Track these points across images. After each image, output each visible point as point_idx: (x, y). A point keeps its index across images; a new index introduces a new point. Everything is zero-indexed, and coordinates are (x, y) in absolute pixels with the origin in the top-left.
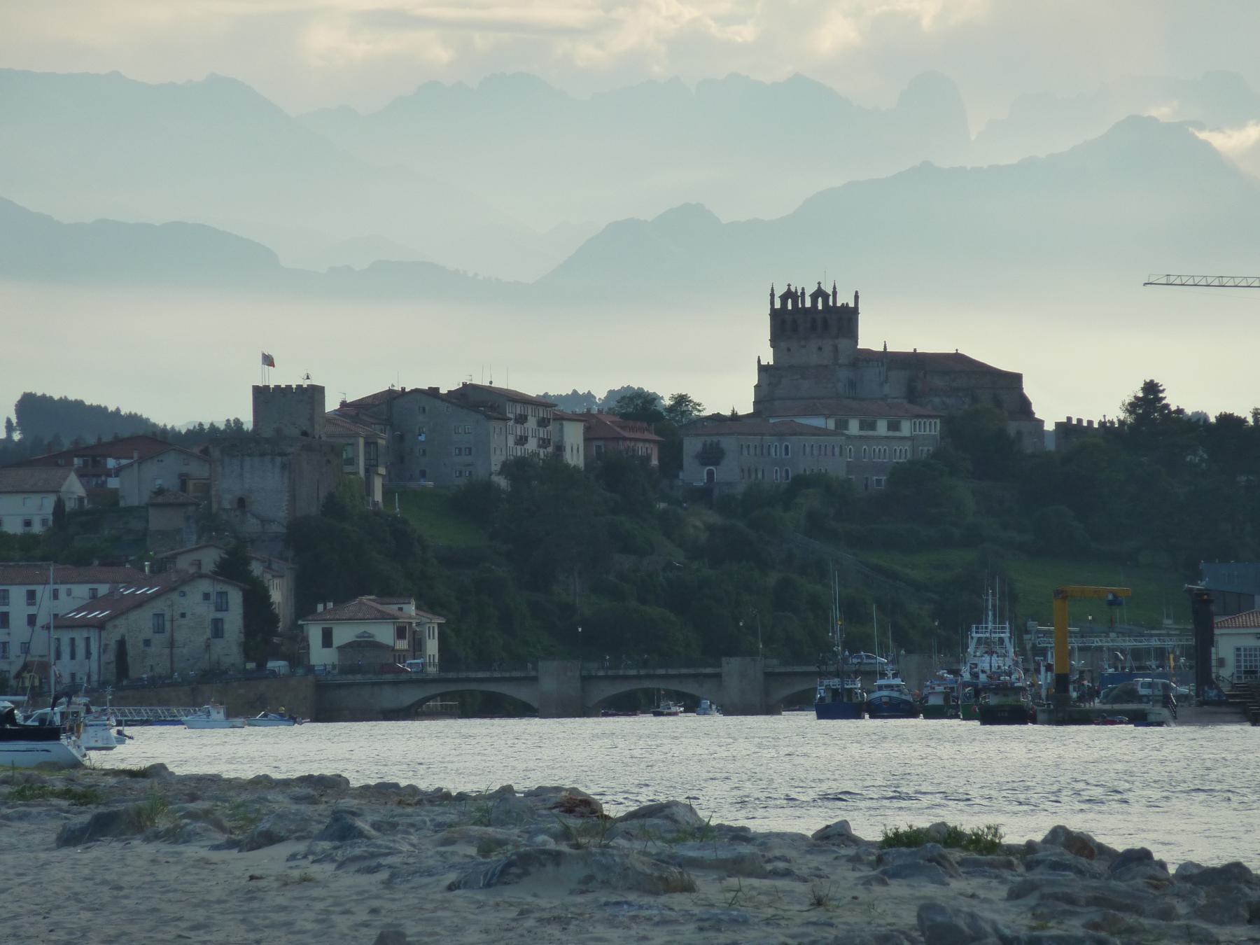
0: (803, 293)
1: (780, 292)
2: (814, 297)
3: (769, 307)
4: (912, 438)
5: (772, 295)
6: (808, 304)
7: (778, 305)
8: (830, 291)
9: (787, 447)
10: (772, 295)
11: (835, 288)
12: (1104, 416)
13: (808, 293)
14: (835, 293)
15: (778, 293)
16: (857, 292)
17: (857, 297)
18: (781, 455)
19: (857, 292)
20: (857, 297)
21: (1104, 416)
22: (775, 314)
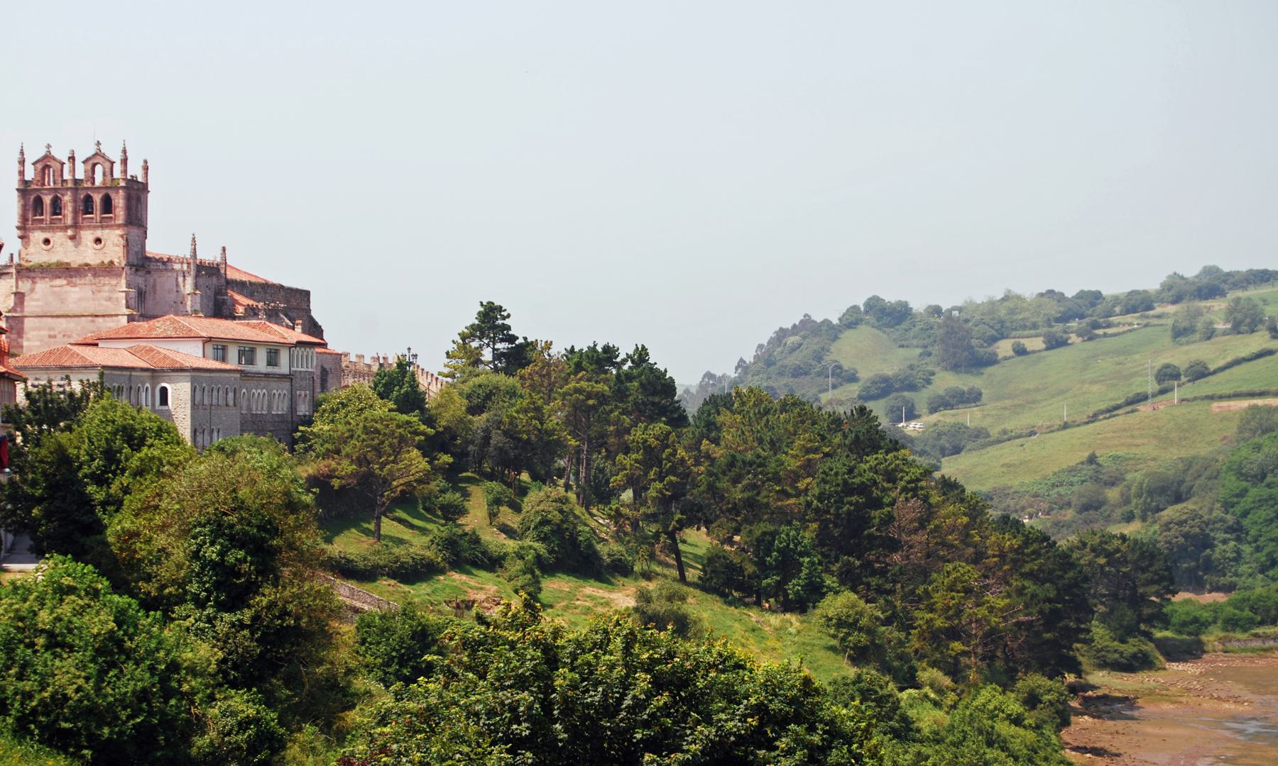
0: (72, 159)
1: (33, 155)
2: (91, 163)
3: (17, 177)
4: (289, 377)
5: (22, 162)
6: (80, 175)
7: (30, 174)
8: (116, 157)
9: (164, 391)
10: (22, 162)
11: (125, 151)
12: (409, 349)
13: (79, 159)
14: (125, 161)
15: (31, 158)
16: (146, 162)
17: (146, 169)
18: (153, 404)
19: (146, 162)
20: (146, 169)
21: (409, 349)
22: (24, 189)
